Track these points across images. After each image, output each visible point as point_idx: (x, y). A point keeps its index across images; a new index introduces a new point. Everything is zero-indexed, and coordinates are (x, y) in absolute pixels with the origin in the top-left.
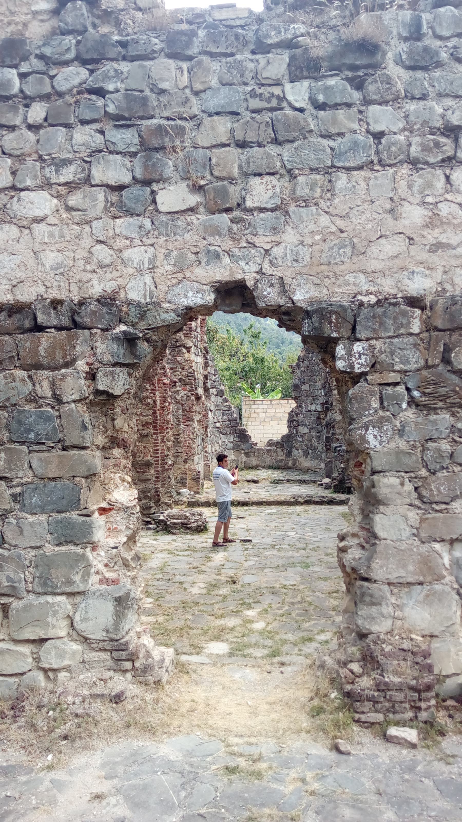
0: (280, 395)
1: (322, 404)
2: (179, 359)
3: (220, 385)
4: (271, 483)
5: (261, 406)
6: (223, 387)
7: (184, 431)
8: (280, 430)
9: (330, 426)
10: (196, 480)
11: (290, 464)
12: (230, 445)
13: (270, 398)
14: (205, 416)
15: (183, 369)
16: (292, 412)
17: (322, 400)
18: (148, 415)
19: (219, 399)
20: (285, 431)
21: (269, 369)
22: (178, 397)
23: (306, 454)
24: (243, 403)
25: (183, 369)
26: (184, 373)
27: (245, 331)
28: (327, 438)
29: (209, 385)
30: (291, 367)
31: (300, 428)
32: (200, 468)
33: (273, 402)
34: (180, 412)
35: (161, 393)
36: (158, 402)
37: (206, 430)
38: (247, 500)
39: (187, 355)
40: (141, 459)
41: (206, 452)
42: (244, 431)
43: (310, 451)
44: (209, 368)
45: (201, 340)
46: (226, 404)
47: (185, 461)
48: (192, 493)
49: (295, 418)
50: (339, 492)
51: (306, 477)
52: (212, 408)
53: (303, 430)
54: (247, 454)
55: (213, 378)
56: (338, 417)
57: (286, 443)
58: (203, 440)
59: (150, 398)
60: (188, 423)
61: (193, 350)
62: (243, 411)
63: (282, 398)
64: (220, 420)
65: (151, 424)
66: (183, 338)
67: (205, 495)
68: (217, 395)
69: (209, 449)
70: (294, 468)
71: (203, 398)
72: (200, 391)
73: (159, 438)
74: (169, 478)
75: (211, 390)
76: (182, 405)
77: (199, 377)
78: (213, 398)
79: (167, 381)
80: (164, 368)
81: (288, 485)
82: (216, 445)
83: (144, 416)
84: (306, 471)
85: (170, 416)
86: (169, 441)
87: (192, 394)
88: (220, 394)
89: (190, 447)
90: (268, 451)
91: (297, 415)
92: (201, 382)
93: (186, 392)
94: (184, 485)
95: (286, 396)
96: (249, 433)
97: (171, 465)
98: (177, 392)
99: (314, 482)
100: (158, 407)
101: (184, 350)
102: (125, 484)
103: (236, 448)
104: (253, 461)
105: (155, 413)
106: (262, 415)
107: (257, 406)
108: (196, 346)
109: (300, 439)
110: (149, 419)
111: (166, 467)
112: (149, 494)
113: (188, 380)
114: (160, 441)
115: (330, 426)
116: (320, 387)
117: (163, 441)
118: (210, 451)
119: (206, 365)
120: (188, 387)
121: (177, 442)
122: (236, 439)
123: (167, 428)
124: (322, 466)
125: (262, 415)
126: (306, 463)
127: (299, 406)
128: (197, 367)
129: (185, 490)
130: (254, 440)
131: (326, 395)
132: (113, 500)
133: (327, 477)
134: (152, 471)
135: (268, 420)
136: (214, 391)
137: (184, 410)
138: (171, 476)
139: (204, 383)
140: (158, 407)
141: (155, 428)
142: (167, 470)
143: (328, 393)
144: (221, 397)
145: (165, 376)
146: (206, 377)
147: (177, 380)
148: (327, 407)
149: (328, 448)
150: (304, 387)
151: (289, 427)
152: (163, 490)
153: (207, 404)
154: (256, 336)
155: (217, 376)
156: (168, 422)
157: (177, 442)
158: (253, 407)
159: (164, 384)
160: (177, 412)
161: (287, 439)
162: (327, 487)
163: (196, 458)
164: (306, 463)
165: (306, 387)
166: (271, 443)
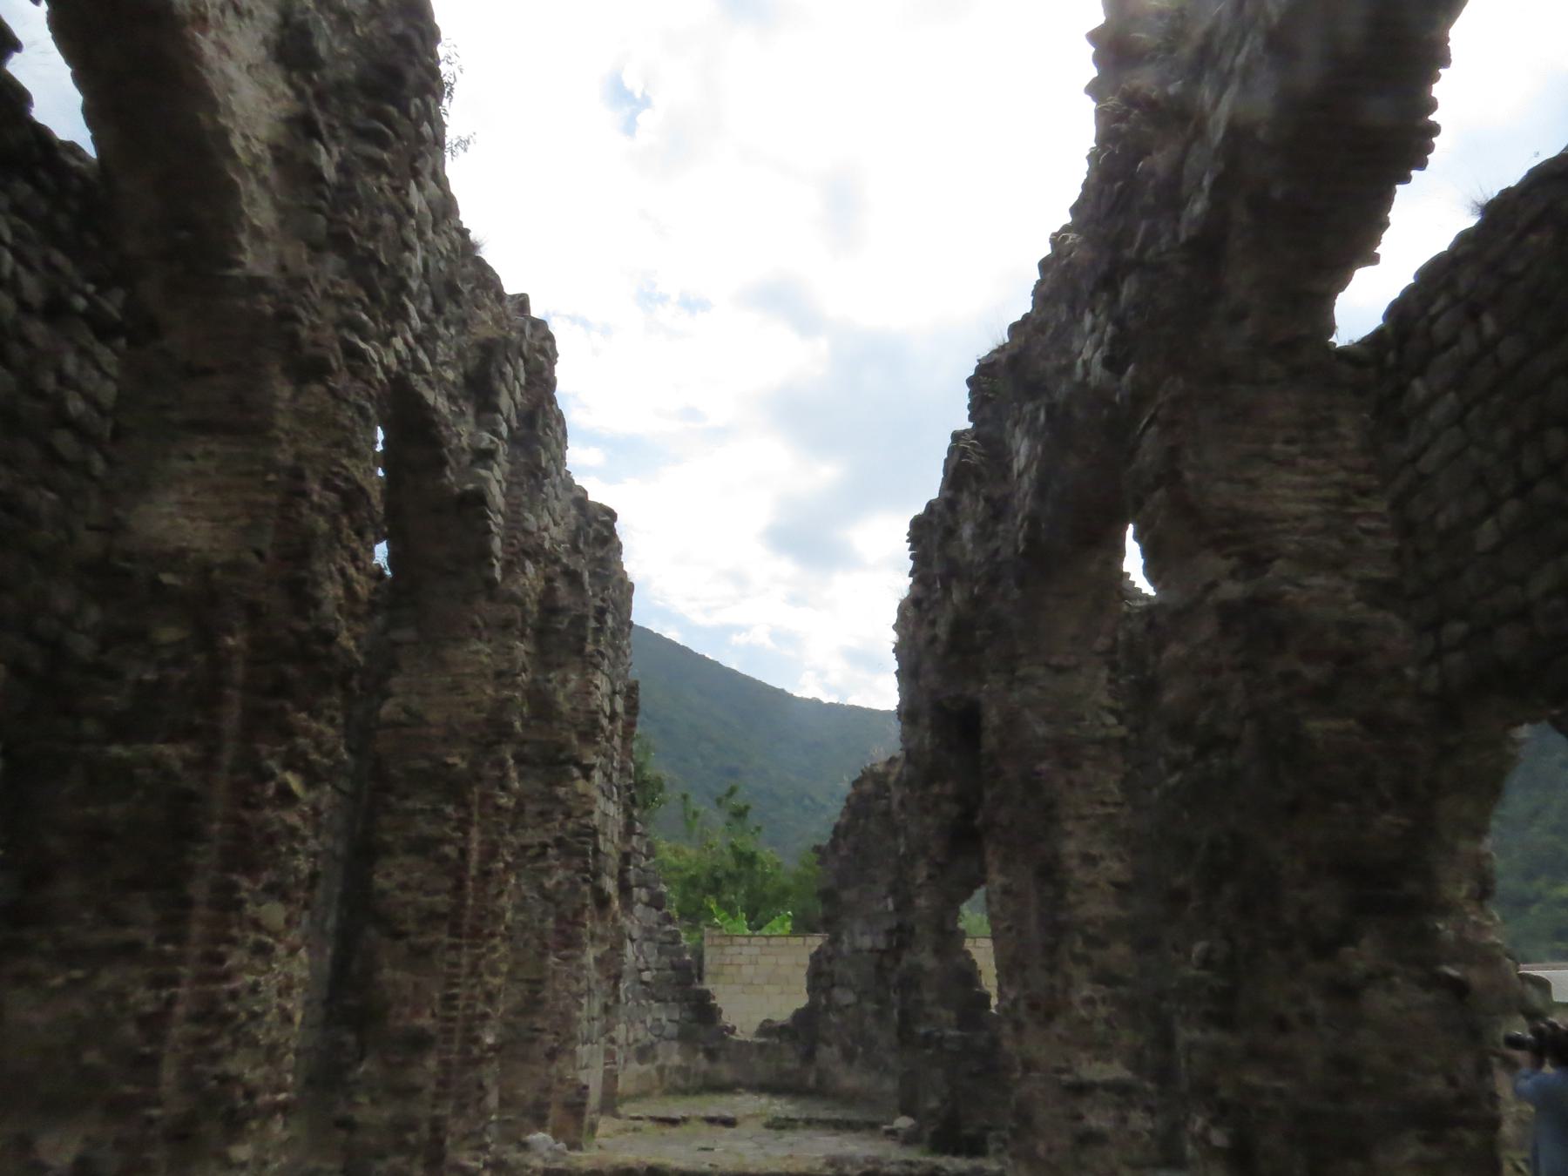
0: (788, 925)
1: (889, 933)
2: (561, 791)
3: (658, 881)
4: (768, 1126)
5: (746, 950)
6: (664, 888)
7: (554, 972)
8: (786, 998)
9: (909, 983)
10: (576, 1108)
11: (811, 1080)
12: (672, 1029)
13: (766, 931)
14: (617, 948)
15: (568, 815)
16: (817, 953)
17: (890, 923)
18: (437, 892)
19: (654, 915)
20: (802, 1000)
21: (765, 877)
22: (549, 883)
23: (848, 1056)
24: (706, 942)
25: (568, 815)
26: (570, 825)
27: (719, 801)
28: (902, 1013)
29: (632, 877)
30: (817, 849)
31: (837, 992)
32: (593, 1078)
33: (773, 941)
34: (550, 923)
35: (484, 831)
36: (474, 858)
37: (616, 985)
38: (706, 1167)
39: (581, 785)
40: (400, 1023)
41: (612, 1041)
42: (706, 996)
43: (860, 1050)
44: (635, 838)
45: (622, 770)
46: (668, 927)
47: (552, 1055)
48: (561, 1146)
49: (825, 967)
50: (944, 1152)
51: (853, 1115)
52: (636, 934)
53: (845, 997)
54: (711, 1055)
55: (643, 863)
56: (928, 960)
57: (802, 1030)
58: (606, 1009)
59: (451, 841)
60: (564, 953)
61: (597, 776)
62: (707, 959)
63: (795, 932)
64: (652, 966)
65: (443, 917)
66: (575, 742)
67: (595, 1152)
68: (647, 905)
69: (620, 1032)
70: (821, 1091)
71: (616, 904)
72: (610, 885)
73: (465, 961)
74: (481, 1086)
75: (636, 890)
76: (558, 905)
77: (610, 845)
78: (639, 909)
79: (504, 800)
80: (501, 764)
81: (809, 1132)
82: (638, 1025)
83: (427, 894)
84: (849, 1099)
85: (504, 901)
86: (495, 972)
87: (585, 881)
88: (656, 902)
89: (567, 1018)
90: (762, 1047)
91: (830, 959)
92: (613, 863)
93: (570, 873)
94: (540, 1122)
95: (803, 926)
96: (720, 1001)
97: (491, 1048)
98: (547, 871)
99: (873, 1126)
100: (473, 872)
101: (576, 772)
103: (685, 1037)
104: (725, 1072)
105: (459, 887)
106: (748, 971)
107: (736, 949)
108: (608, 777)
109: (834, 1018)
110: (442, 902)
111: (476, 1051)
112: (411, 1137)
113: (579, 844)
114: (465, 970)
115: (909, 983)
116: (884, 890)
117: (474, 971)
118: (621, 1040)
119: (629, 830)
120: (577, 862)
121: (533, 1003)
122: (688, 1015)
123: (492, 935)
124: (890, 1085)
125: (748, 971)
126: (849, 1079)
127: (835, 940)
128: (605, 824)
129: (540, 1136)
130: (727, 1019)
131: (897, 909)
133: (906, 1111)
134: (431, 1063)
135: (762, 980)
137: (560, 918)
138: (488, 1082)
139: (623, 872)
140: (473, 872)
141: (455, 930)
142: (478, 1062)
143: (904, 904)
144: (659, 908)
145: (504, 788)
146: (626, 858)
147: (550, 841)
148: (901, 937)
149: (904, 1035)
151: (812, 989)
152: (457, 1126)
153: (624, 921)
154: (740, 814)
155: (652, 860)
156: (498, 916)
157: (533, 1003)
158: (729, 950)
159: (498, 808)
160: (542, 921)
161: (804, 1018)
162: (910, 1139)
163: (582, 1050)
164: (849, 1079)
165: (848, 895)
166: (767, 1029)
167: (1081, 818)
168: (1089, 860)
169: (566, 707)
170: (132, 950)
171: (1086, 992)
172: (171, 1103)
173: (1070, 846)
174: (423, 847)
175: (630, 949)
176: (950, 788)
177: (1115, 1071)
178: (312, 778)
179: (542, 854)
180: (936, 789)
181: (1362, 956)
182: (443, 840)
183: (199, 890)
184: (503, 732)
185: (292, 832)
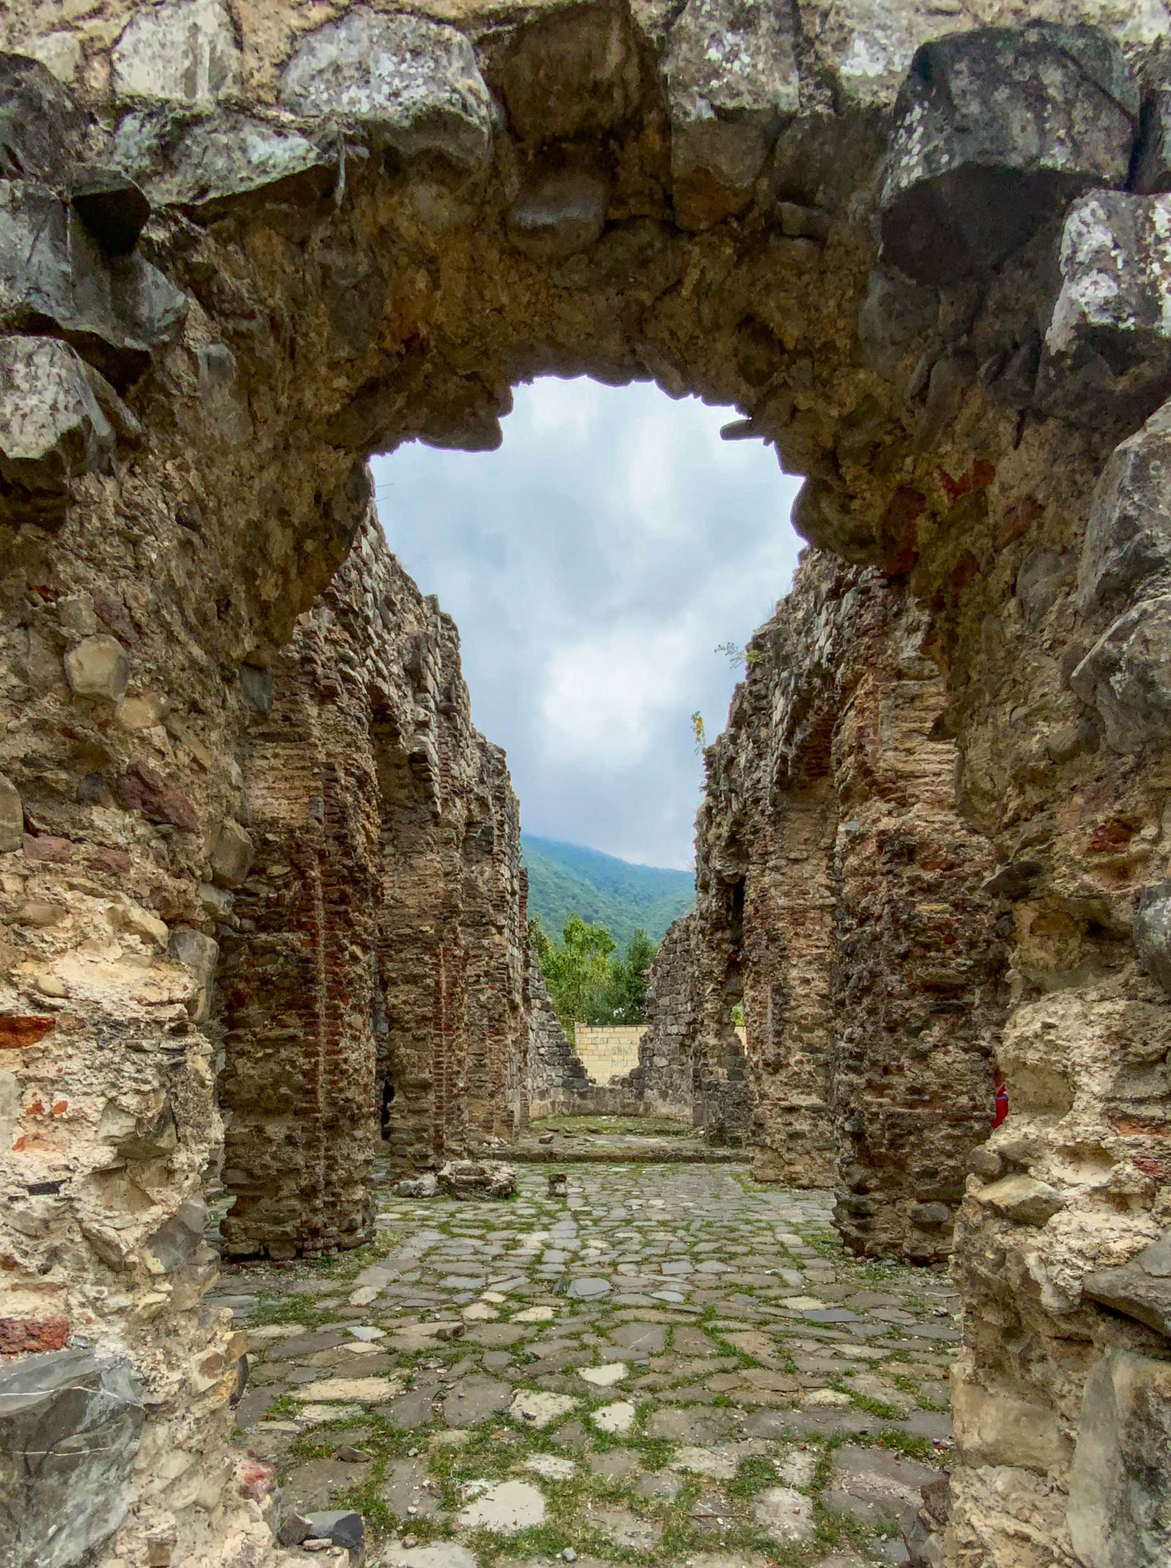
8: (629, 1063)
14: (524, 1034)
19: (545, 1016)
22: (483, 998)
34: (485, 1021)
39: (497, 938)
72: (518, 998)
77: (517, 974)
80: (454, 930)
88: (546, 1007)
92: (519, 985)
96: (585, 1065)
98: (481, 991)
102: (134, 940)
113: (499, 975)
132: (49, 983)
136: (538, 1003)
150: (664, 1001)
151: (641, 1060)
167: (801, 956)
168: (807, 981)
169: (484, 889)
170: (293, 1039)
171: (798, 1056)
172: (325, 1113)
173: (794, 973)
174: (414, 980)
175: (531, 1035)
176: (728, 934)
177: (814, 1100)
178: (365, 948)
179: (477, 982)
180: (719, 935)
181: (935, 1033)
182: (425, 976)
183: (319, 1008)
184: (454, 911)
185: (360, 977)
